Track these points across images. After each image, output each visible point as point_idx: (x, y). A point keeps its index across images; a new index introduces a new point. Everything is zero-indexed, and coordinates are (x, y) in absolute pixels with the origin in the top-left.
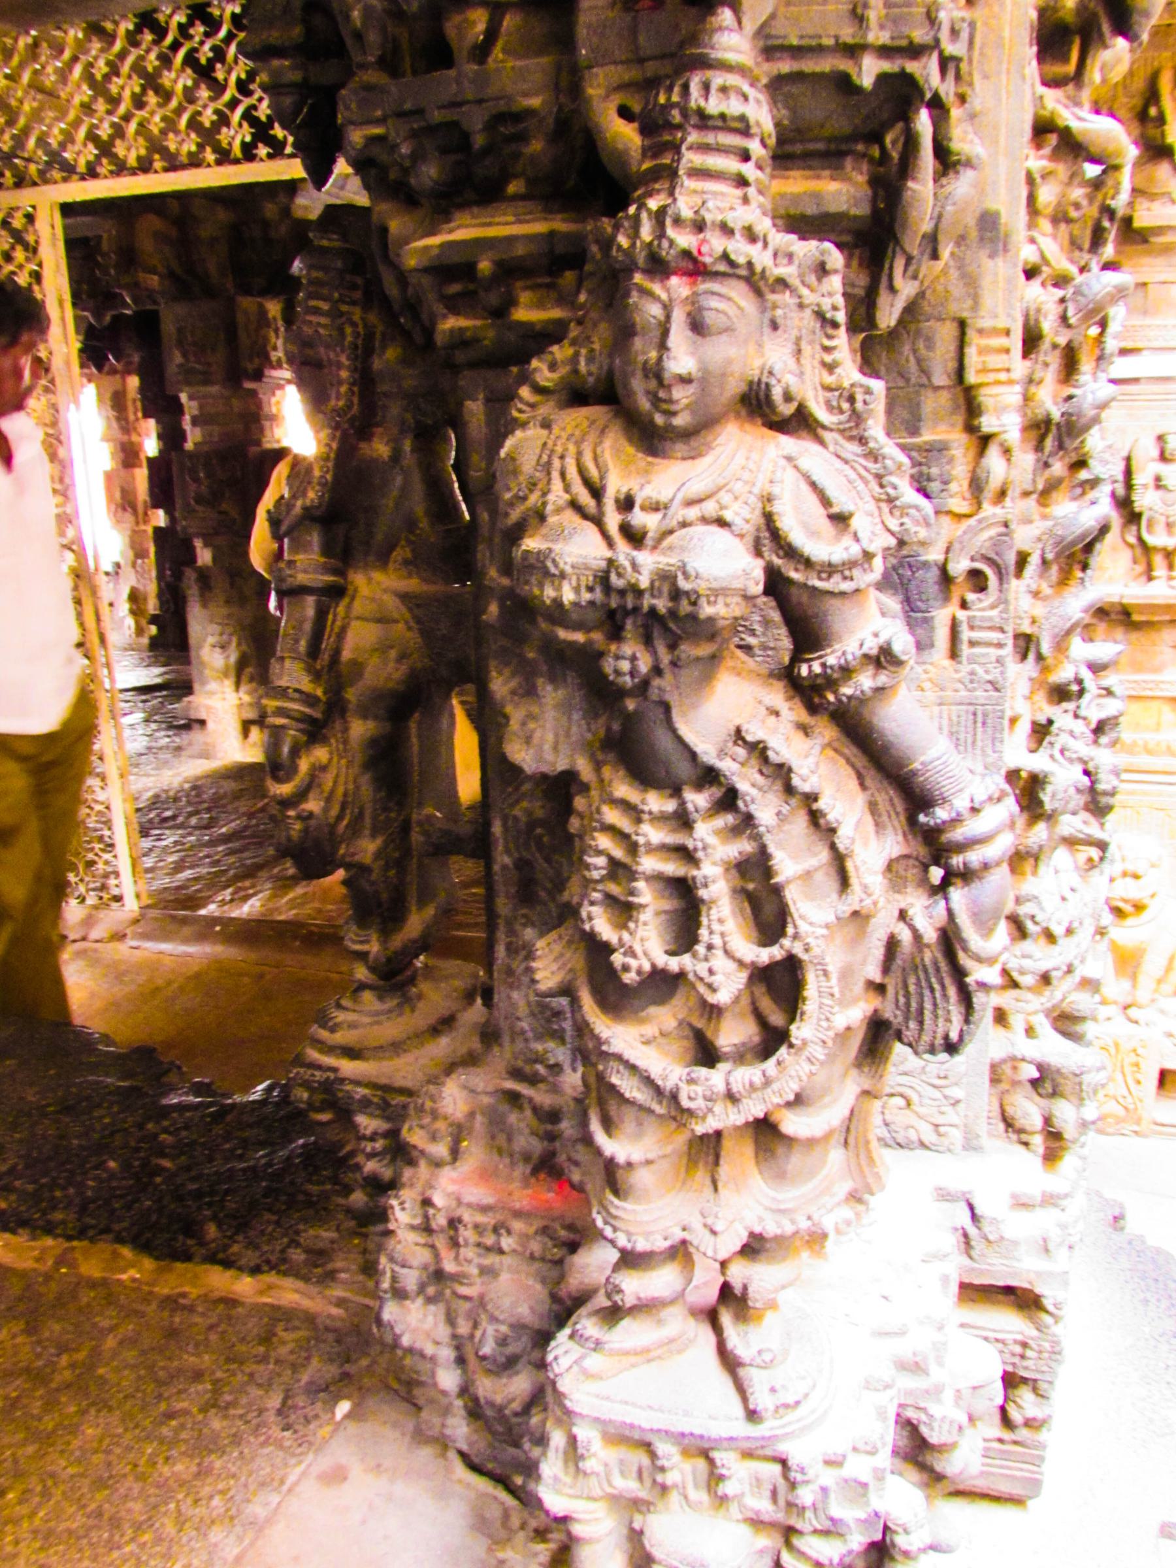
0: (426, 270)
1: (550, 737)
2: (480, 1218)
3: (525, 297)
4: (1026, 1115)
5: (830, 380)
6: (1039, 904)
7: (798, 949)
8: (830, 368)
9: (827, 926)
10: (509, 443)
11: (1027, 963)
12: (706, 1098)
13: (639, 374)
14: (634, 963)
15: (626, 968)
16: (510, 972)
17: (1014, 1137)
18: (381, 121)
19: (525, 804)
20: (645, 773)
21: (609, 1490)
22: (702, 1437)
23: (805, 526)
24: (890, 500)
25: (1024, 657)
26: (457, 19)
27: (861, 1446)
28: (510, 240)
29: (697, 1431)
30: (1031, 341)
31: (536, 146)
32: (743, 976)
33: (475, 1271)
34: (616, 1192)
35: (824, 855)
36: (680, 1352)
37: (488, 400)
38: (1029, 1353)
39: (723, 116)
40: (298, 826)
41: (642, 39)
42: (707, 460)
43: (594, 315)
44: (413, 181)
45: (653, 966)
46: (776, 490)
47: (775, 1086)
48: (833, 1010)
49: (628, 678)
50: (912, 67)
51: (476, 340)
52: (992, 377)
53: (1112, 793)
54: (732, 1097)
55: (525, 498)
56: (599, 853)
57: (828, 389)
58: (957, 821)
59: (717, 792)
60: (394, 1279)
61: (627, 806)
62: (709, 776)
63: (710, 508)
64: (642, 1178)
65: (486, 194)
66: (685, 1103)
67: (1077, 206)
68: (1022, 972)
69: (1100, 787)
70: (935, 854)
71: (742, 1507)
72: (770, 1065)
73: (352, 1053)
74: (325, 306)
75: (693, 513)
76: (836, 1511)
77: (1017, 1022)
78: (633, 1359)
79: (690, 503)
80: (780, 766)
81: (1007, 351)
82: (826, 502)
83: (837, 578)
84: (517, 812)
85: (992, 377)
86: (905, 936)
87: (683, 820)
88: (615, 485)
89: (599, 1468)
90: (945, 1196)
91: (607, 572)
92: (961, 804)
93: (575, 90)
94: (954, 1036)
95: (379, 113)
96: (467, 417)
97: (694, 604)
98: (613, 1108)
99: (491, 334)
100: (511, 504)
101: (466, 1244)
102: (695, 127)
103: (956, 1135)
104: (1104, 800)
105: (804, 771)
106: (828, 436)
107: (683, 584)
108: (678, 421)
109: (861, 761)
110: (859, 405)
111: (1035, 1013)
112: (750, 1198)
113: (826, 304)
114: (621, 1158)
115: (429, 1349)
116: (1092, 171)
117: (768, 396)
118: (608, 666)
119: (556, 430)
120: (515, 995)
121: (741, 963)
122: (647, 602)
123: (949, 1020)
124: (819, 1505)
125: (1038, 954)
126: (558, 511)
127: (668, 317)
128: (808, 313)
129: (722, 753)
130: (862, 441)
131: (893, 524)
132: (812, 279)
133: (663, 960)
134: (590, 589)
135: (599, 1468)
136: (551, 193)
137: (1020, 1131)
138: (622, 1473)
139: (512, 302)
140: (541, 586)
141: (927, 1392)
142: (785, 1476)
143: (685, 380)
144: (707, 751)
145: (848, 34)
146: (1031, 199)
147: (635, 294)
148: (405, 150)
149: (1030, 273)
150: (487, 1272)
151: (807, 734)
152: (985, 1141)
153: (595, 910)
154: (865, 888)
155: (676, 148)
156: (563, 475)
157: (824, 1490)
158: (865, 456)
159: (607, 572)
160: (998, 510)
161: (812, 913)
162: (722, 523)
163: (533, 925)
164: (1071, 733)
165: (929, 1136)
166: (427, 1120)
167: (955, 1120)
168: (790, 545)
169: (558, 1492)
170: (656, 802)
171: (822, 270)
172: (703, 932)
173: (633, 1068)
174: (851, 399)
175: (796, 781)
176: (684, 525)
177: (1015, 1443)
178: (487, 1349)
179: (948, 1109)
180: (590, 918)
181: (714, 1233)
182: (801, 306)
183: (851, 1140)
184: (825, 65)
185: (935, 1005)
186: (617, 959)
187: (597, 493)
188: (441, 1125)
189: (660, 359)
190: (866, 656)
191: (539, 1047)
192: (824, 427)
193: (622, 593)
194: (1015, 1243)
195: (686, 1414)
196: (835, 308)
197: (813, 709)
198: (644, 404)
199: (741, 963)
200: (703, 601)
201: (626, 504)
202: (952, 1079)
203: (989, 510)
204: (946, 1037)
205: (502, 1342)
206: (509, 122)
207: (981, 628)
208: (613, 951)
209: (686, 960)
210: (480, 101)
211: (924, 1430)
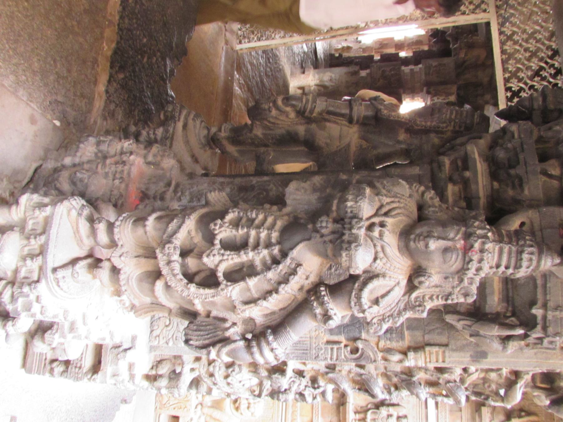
0: (466, 153)
1: (298, 197)
2: (126, 172)
3: (456, 188)
5: (427, 298)
7: (222, 286)
8: (431, 298)
9: (230, 297)
10: (404, 183)
11: (217, 369)
12: (169, 253)
13: (429, 229)
14: (217, 227)
15: (215, 225)
16: (214, 183)
17: (155, 364)
19: (274, 188)
20: (284, 231)
21: (28, 219)
22: (47, 252)
23: (374, 289)
24: (383, 320)
25: (327, 367)
27: (44, 309)
28: (477, 183)
30: (441, 370)
31: (511, 192)
33: (107, 170)
34: (135, 221)
35: (256, 296)
36: (78, 244)
37: (419, 175)
38: (77, 369)
39: (521, 259)
40: (266, 107)
41: (549, 230)
44: (498, 148)
45: (216, 234)
46: (387, 279)
47: (173, 278)
48: (200, 298)
49: (319, 225)
50: (539, 327)
51: (441, 171)
53: (278, 399)
54: (169, 262)
55: (384, 188)
56: (257, 215)
57: (424, 297)
58: (268, 343)
59: (279, 257)
60: (104, 141)
62: (284, 254)
63: (381, 255)
64: (140, 231)
65: (494, 175)
66: (167, 246)
67: (489, 386)
68: (214, 367)
69: (281, 395)
70: (257, 335)
71: (22, 266)
72: (181, 276)
73: (185, 126)
74: (453, 117)
75: (379, 249)
76: (20, 300)
77: (196, 365)
78: (75, 228)
79: (383, 248)
81: (437, 361)
82: (383, 296)
83: (355, 300)
84: (272, 185)
86: (227, 325)
87: (268, 245)
88: (389, 221)
90: (134, 339)
91: (358, 218)
92: (275, 345)
93: (531, 206)
94: (191, 342)
95: (522, 136)
97: (346, 249)
98: (165, 220)
99: (443, 176)
100: (382, 183)
101: (116, 167)
103: (155, 343)
104: (276, 396)
105: (286, 289)
106: (406, 297)
107: (353, 245)
108: (412, 243)
109: (290, 309)
110: (417, 308)
111: (199, 372)
112: (132, 269)
113: (454, 296)
115: (79, 154)
116: (502, 392)
117: (421, 276)
118: (324, 218)
119: (408, 200)
120: (206, 185)
121: (217, 266)
122: (347, 232)
123: (197, 340)
124: (22, 294)
125: (220, 373)
126: (380, 200)
127: (449, 240)
128: (451, 290)
129: (292, 259)
130: (405, 309)
131: (375, 321)
132: (463, 291)
133: (219, 237)
134: (351, 212)
135: (36, 215)
137: (157, 366)
138: (34, 223)
139: (454, 183)
140: (353, 194)
141: (63, 333)
143: (427, 246)
145: (551, 304)
146: (492, 370)
147: (458, 228)
149: (465, 370)
150: (106, 175)
151: (299, 289)
152: (153, 354)
153: (237, 213)
154: (244, 310)
155: (510, 243)
156: (392, 202)
157: (28, 296)
159: (358, 218)
160: (380, 358)
161: (235, 292)
162: (375, 259)
163: (231, 191)
164: (300, 384)
165: (155, 333)
166: (161, 153)
167: (161, 343)
169: (27, 200)
170: (275, 235)
171: (466, 295)
172: (228, 252)
173: (180, 227)
174: (420, 306)
175: (283, 286)
176: (375, 246)
177: (45, 364)
178: (78, 175)
179: (165, 340)
180: (233, 212)
181: (120, 256)
182: (453, 287)
183: (154, 305)
184: (540, 296)
185: (202, 336)
186: (219, 222)
187: (386, 214)
188: (159, 158)
189: (434, 237)
190: (328, 311)
191: (187, 193)
192: (410, 296)
193: (350, 223)
194: (117, 364)
196: (452, 300)
197: (309, 291)
198: (418, 231)
199: (217, 266)
200: (347, 252)
201: (382, 225)
202: (176, 342)
203: (380, 355)
204: (191, 340)
205: (81, 180)
206: (519, 183)
207: (337, 352)
208: (221, 220)
209: (219, 246)
210: (527, 172)
211: (49, 332)
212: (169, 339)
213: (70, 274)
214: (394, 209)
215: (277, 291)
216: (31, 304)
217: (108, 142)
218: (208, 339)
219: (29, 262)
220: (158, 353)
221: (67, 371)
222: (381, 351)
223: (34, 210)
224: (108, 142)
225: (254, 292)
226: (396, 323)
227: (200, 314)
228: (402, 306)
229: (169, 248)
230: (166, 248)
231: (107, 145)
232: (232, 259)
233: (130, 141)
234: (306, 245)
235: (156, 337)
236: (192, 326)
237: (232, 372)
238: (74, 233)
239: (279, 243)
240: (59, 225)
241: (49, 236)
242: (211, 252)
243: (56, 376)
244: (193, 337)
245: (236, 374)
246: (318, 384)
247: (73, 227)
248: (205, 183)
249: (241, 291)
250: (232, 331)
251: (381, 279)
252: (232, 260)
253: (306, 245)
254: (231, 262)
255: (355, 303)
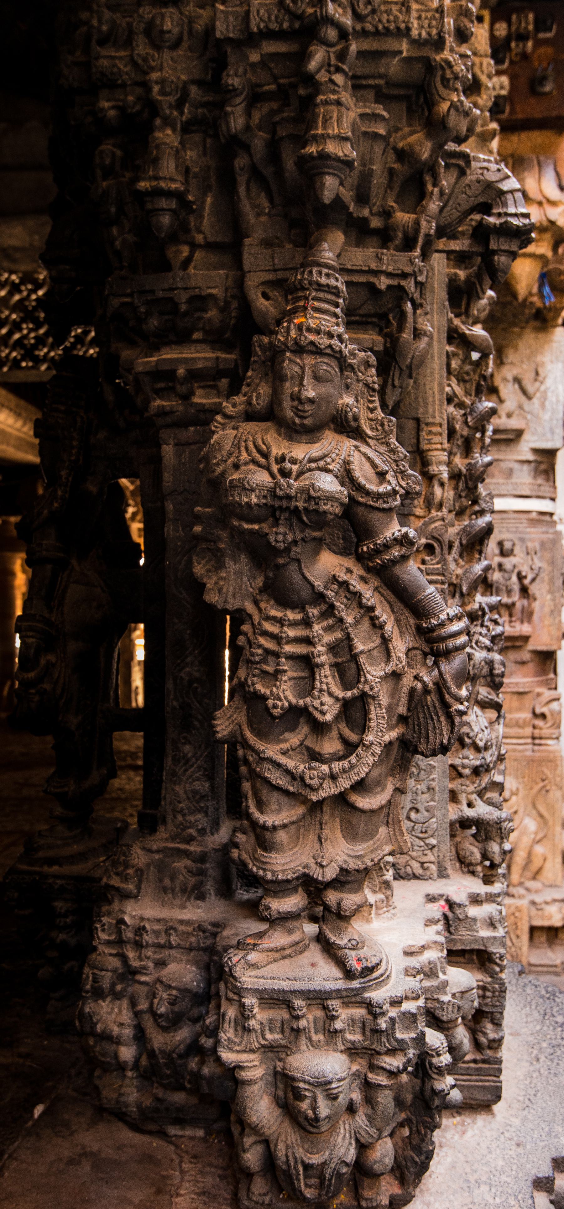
0: (147, 373)
1: (231, 589)
2: (156, 927)
3: (199, 392)
4: (472, 853)
5: (371, 416)
6: (470, 726)
7: (367, 688)
8: (372, 410)
9: (381, 678)
10: (215, 437)
11: (466, 761)
12: (319, 778)
13: (289, 399)
14: (279, 703)
15: (275, 707)
16: (174, 774)
17: (466, 870)
18: (131, 295)
19: (188, 669)
20: (284, 603)
21: (263, 1042)
22: (320, 991)
23: (364, 476)
24: (402, 472)
25: (453, 596)
26: (174, 249)
27: (410, 995)
28: (195, 360)
29: (318, 988)
30: (451, 433)
31: (212, 313)
32: (337, 707)
33: (151, 965)
34: (265, 849)
35: (378, 641)
36: (301, 952)
37: (176, 445)
38: (488, 994)
39: (328, 285)
40: (36, 698)
41: (276, 261)
42: (317, 445)
43: (257, 381)
44: (144, 327)
45: (290, 704)
46: (351, 459)
47: (356, 770)
48: (381, 733)
49: (282, 544)
50: (403, 283)
51: (172, 412)
52: (434, 446)
53: (503, 675)
54: (333, 777)
55: (226, 461)
56: (260, 646)
57: (371, 420)
58: (442, 625)
59: (324, 607)
60: (95, 980)
61: (275, 619)
62: (319, 597)
63: (322, 463)
64: (282, 836)
65: (183, 338)
66: (308, 781)
67: (468, 373)
68: (464, 766)
69: (496, 672)
70: (432, 644)
71: (344, 1039)
72: (353, 759)
73: (51, 862)
74: (63, 408)
75: (313, 465)
76: (399, 1035)
77: (463, 798)
78: (277, 955)
79: (311, 461)
80: (355, 593)
81: (441, 434)
82: (374, 465)
83: (381, 501)
84: (182, 674)
85: (434, 446)
86: (419, 686)
87: (307, 623)
88: (276, 451)
89: (257, 1027)
90: (431, 899)
91: (275, 488)
92: (443, 616)
93: (240, 283)
94: (445, 741)
95: (129, 291)
96: (163, 454)
97: (317, 504)
98: (264, 792)
99: (181, 408)
100: (217, 464)
101: (147, 945)
102: (315, 290)
103: (433, 868)
104: (497, 679)
105: (368, 596)
106: (371, 442)
107: (312, 493)
108: (306, 422)
109: (392, 598)
110: (386, 428)
111: (472, 793)
112: (340, 852)
113: (370, 380)
114: (269, 823)
115: (116, 1030)
116: (475, 356)
117: (346, 416)
118: (272, 538)
119: (241, 430)
120: (177, 788)
121: (337, 699)
122: (293, 504)
123: (442, 734)
124: (390, 1032)
125: (471, 757)
126: (246, 464)
127: (303, 372)
128: (361, 384)
129: (326, 587)
130: (388, 444)
131: (403, 484)
132: (362, 368)
133: (294, 701)
134: (265, 497)
135: (257, 1027)
136: (215, 339)
137: (470, 864)
138: (271, 1030)
139: (192, 393)
140: (240, 495)
141: (438, 988)
142: (370, 1012)
143: (311, 401)
144: (319, 584)
145: (374, 266)
146: (448, 365)
147: (287, 361)
148: (142, 309)
149: (450, 400)
150: (161, 964)
151: (366, 583)
152: (450, 871)
153: (255, 679)
154: (399, 659)
155: (306, 298)
156: (247, 449)
157: (393, 1020)
158: (389, 452)
159: (275, 488)
160: (439, 514)
161: (374, 672)
162: (327, 471)
163: (190, 743)
164: (481, 634)
165: (419, 871)
166: (121, 869)
167: (432, 859)
168: (359, 484)
169: (231, 1050)
170: (292, 615)
171: (368, 365)
172: (318, 683)
173: (278, 765)
174: (382, 425)
175: (364, 600)
176: (310, 470)
177: (484, 1061)
178: (162, 1010)
179: (428, 852)
180: (253, 684)
181: (322, 866)
182: (358, 381)
183: (390, 821)
184: (363, 279)
185: (434, 728)
186: (270, 702)
187: (266, 456)
188: (131, 871)
189: (300, 391)
190: (395, 539)
191: (192, 818)
192: (370, 437)
193: (281, 498)
194: (474, 920)
195: (310, 979)
196: (374, 383)
197: (368, 570)
198: (290, 414)
199: (337, 699)
200: (322, 503)
201: (281, 459)
202: (430, 833)
203: (434, 513)
204: (442, 743)
205: (172, 1003)
206: (201, 301)
207: (432, 574)
208: (267, 699)
209: (308, 700)
210: (186, 289)
211: (438, 1013)
212: (427, 845)
213: (353, 953)
214: (256, 447)
215: (372, 609)
216: (404, 1014)
217: (97, 972)
218: (438, 717)
219: (338, 1025)
220: (448, 864)
221: (492, 1013)
222: (430, 512)
223: (249, 1031)
224: (97, 972)
225: (372, 645)
226: (406, 456)
227: (403, 734)
228: (383, 449)
229: (311, 778)
230: (312, 782)
231: (104, 973)
232: (326, 677)
233: (97, 929)
234: (307, 567)
235: (425, 869)
236: (422, 747)
237: (469, 738)
238: (284, 958)
239: (303, 609)
240: (274, 978)
241: (295, 992)
242: (316, 709)
243: (501, 1034)
244: (438, 741)
245: (472, 730)
246: (477, 611)
247: (275, 961)
248: (173, 790)
249: (372, 665)
250: (426, 679)
251: (352, 466)
252: (327, 678)
253: (307, 567)
254: (330, 680)
255: (385, 502)
